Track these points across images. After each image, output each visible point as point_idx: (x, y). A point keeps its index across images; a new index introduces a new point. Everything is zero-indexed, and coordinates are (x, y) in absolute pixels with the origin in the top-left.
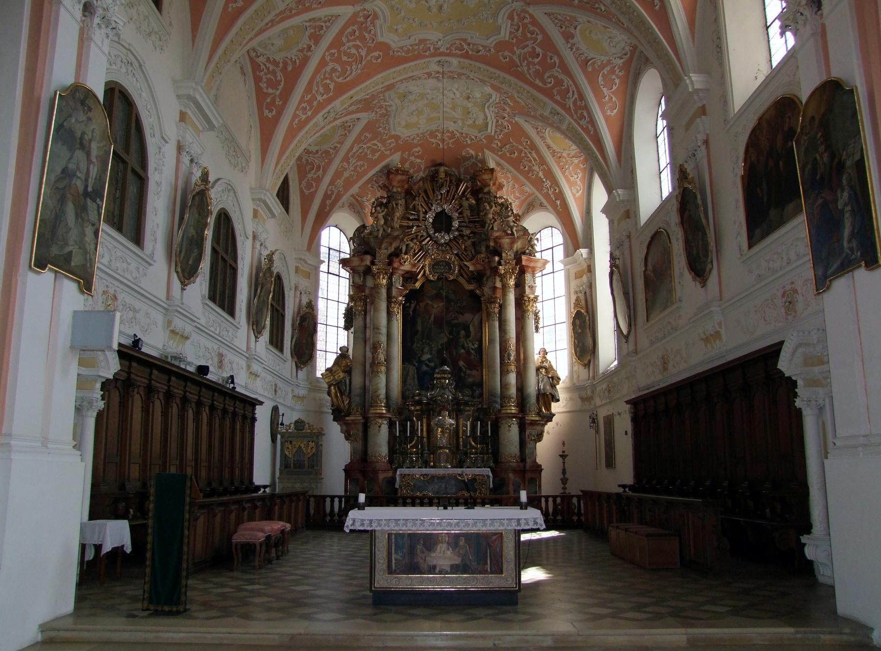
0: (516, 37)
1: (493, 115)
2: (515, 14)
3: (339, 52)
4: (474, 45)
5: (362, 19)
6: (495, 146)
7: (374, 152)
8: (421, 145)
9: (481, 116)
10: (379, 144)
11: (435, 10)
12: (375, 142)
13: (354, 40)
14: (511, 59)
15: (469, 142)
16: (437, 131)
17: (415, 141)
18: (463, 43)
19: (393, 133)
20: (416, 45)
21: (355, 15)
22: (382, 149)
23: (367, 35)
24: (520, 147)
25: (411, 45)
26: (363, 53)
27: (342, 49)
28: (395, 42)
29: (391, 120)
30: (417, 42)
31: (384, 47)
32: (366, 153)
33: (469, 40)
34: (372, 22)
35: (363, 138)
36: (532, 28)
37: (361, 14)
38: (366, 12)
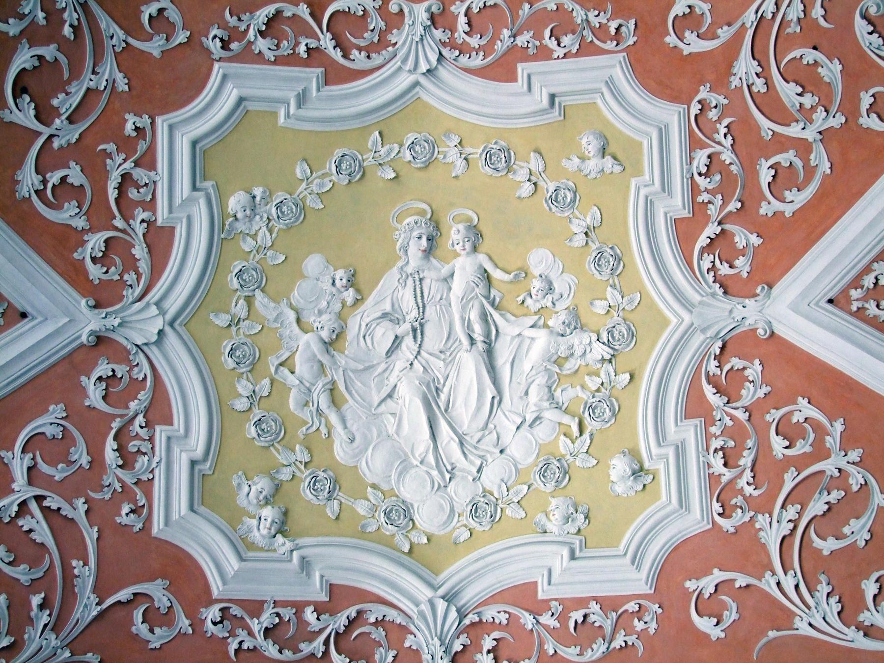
0: (126, 145)
2: (144, 266)
3: (850, 109)
4: (292, 60)
5: (743, 237)
11: (455, 234)
13: (781, 143)
14: (132, 27)
18: (337, 55)
20: (523, 54)
21: (767, 274)
23: (727, 157)
25: (544, 54)
26: (745, 66)
27: (838, 121)
28: (610, 83)
30: (522, 69)
31: (663, 74)
33: (315, 73)
34: (699, 211)
36: (68, 214)
37: (742, 264)
38: (724, 269)
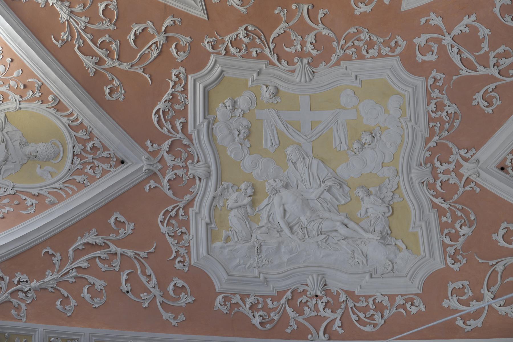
1: (195, 149)
6: (184, 40)
7: (469, 41)
8: (353, 20)
9: (220, 132)
10: (456, 60)
12: (464, 72)
15: (242, 32)
16: (314, 63)
17: (365, 36)
19: (419, 82)
22: (447, 40)
24: (125, 66)
29: (423, 130)
32: (493, 47)
35: (497, 102)
